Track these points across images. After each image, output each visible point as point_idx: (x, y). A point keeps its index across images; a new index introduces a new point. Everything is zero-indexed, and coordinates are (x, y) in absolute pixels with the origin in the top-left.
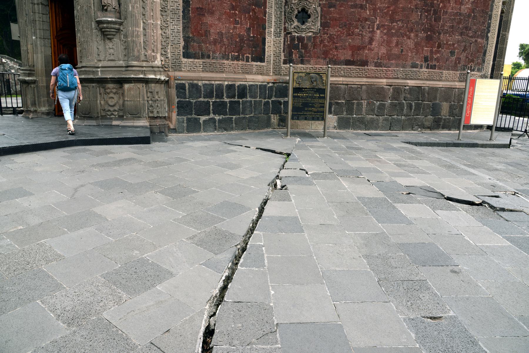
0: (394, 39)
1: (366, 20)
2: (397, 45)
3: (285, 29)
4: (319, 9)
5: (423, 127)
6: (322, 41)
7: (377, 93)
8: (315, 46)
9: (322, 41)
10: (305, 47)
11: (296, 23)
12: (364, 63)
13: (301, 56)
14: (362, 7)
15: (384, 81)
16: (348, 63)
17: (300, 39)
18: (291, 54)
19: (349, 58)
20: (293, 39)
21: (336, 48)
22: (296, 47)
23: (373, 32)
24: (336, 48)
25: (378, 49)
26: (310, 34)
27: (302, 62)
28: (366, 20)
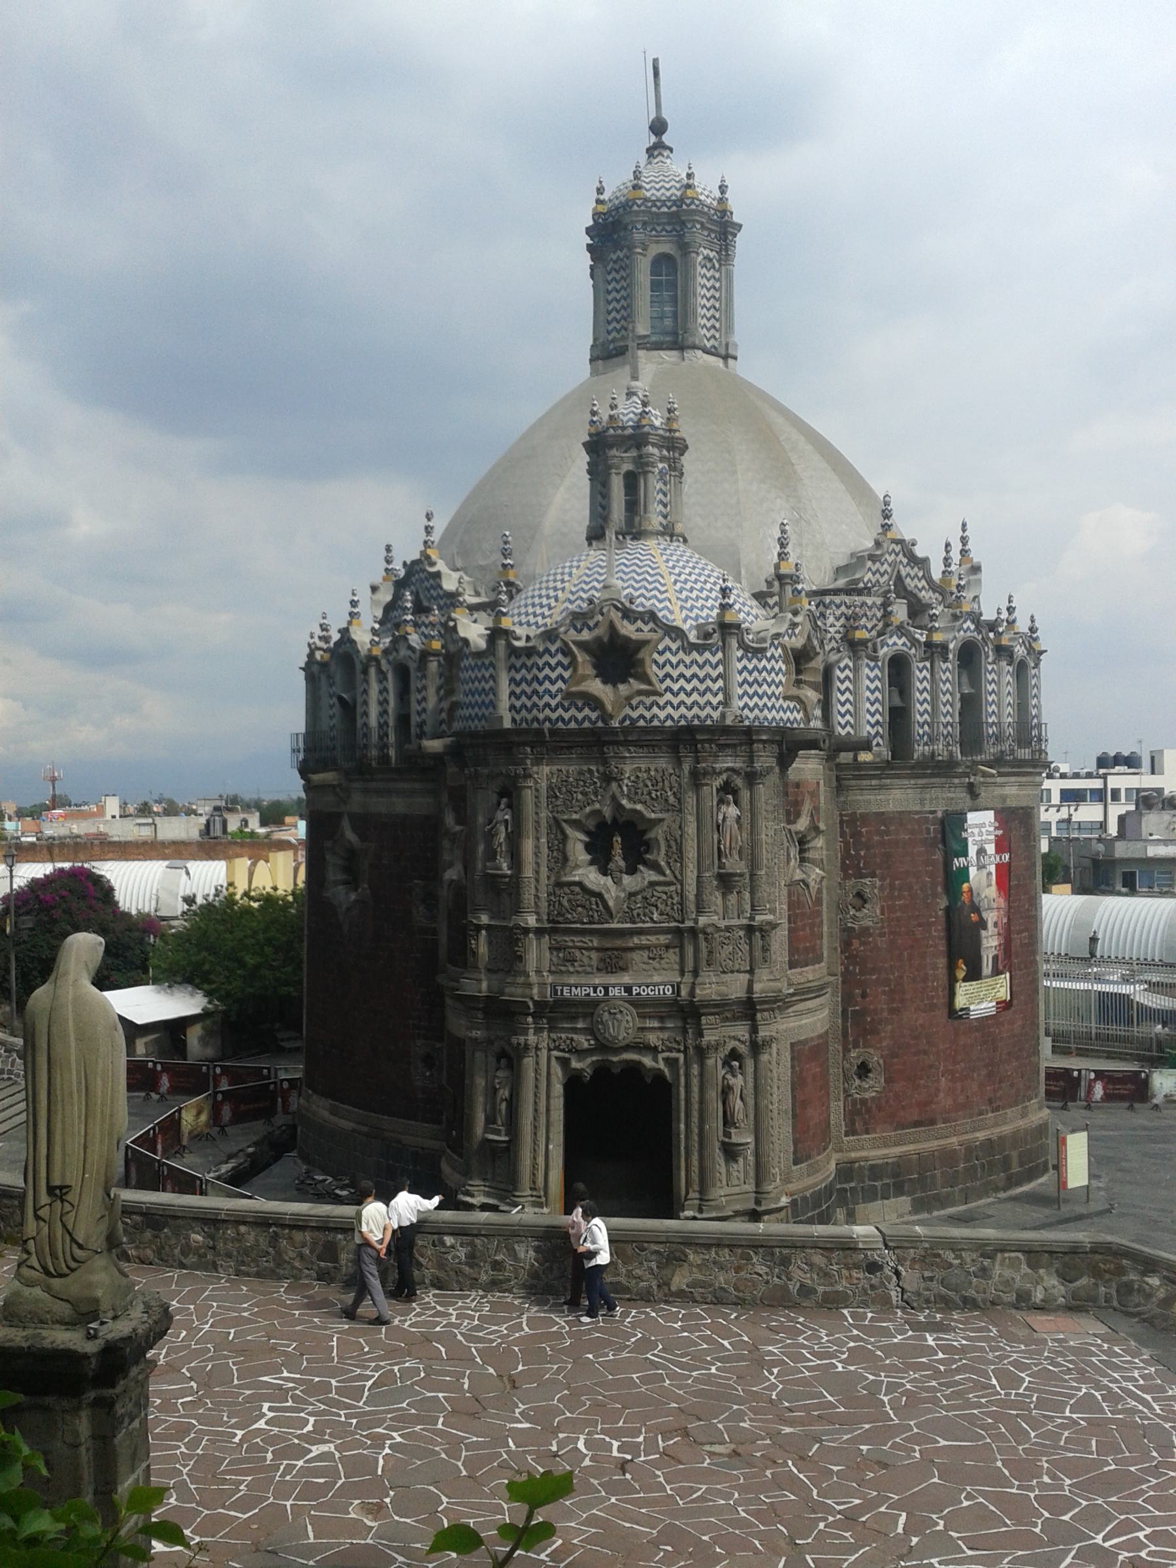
0: (959, 1085)
1: (931, 1067)
2: (962, 1091)
3: (845, 1090)
4: (881, 1061)
5: (997, 1189)
6: (887, 1102)
7: (948, 1157)
8: (880, 1109)
9: (887, 1102)
10: (869, 1111)
11: (858, 1082)
12: (932, 1122)
13: (866, 1123)
14: (925, 1053)
15: (954, 1140)
16: (917, 1124)
17: (864, 1102)
18: (853, 1122)
19: (916, 1118)
20: (854, 1102)
21: (903, 1108)
22: (859, 1113)
23: (938, 1081)
24: (903, 1108)
25: (944, 1100)
26: (874, 1094)
27: (867, 1133)
28: (931, 1067)
